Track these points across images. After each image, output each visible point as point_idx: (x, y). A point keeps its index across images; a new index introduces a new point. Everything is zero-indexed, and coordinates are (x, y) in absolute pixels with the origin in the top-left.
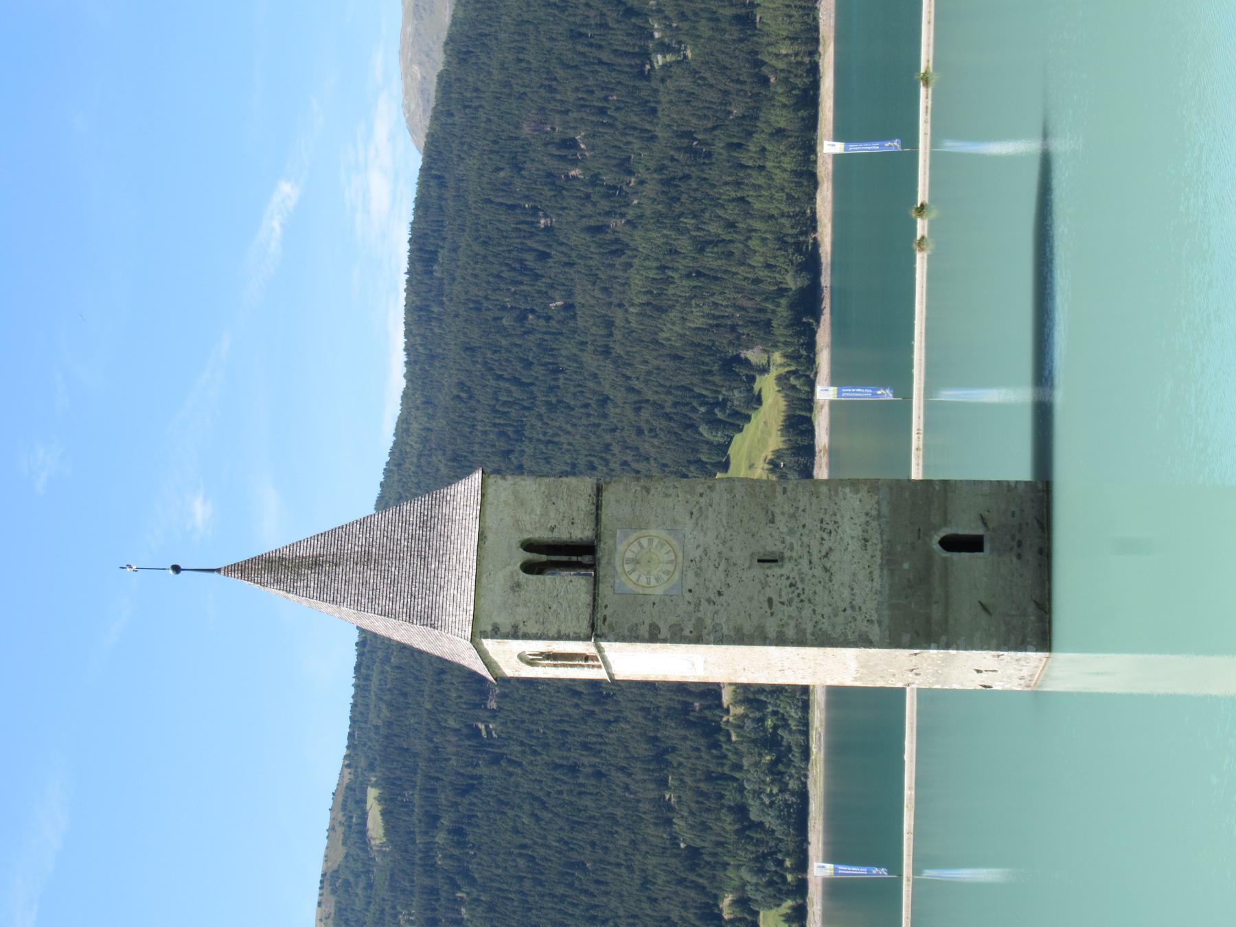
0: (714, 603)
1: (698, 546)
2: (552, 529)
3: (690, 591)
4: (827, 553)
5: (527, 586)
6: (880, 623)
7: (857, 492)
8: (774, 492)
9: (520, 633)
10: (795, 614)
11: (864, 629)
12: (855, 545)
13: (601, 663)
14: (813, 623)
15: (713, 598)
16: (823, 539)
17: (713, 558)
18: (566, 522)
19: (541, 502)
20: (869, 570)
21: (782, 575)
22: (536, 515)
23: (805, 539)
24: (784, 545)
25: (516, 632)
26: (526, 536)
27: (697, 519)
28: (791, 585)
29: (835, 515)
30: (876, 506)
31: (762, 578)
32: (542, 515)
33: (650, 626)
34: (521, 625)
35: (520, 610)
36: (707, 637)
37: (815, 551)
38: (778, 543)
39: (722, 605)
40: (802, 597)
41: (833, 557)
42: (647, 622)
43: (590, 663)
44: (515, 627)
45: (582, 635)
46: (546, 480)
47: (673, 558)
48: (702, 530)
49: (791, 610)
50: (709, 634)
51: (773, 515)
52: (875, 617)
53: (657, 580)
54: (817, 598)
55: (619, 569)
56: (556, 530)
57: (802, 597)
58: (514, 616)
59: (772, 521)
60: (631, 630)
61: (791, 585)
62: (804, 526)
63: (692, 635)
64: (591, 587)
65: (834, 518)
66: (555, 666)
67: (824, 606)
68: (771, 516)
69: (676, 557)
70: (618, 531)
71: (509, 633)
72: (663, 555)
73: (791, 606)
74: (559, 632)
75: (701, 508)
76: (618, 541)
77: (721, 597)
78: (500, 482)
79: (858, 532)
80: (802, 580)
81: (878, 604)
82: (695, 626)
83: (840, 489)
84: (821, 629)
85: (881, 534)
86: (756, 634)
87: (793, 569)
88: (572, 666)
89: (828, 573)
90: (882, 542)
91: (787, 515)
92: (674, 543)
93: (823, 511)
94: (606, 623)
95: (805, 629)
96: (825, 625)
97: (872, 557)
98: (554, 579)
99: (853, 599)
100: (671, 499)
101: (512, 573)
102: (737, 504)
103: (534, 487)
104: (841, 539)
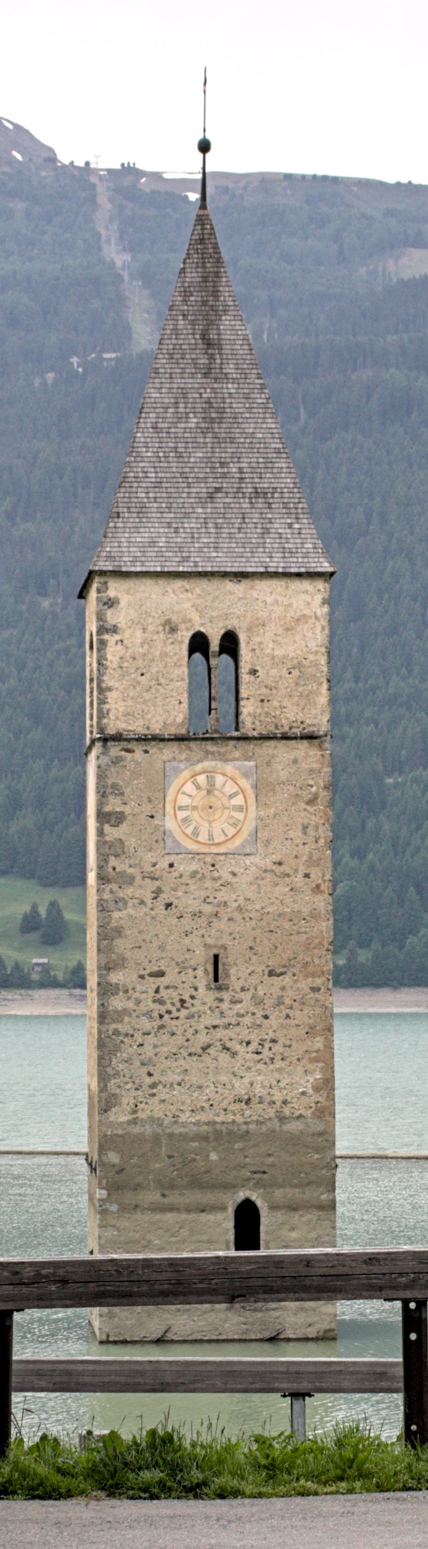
0: (155, 898)
1: (234, 874)
2: (253, 672)
3: (171, 865)
4: (228, 1049)
5: (172, 643)
6: (134, 1122)
7: (317, 1089)
8: (313, 975)
9: (106, 637)
10: (143, 1008)
11: (125, 1101)
12: (240, 1087)
14: (131, 1032)
15: (162, 896)
16: (248, 1043)
17: (219, 895)
18: (264, 691)
19: (291, 655)
20: (206, 1105)
21: (196, 989)
22: (273, 649)
23: (247, 1020)
24: (239, 990)
25: (107, 631)
26: (242, 638)
27: (272, 871)
28: (182, 1001)
29: (283, 1059)
30: (297, 1113)
31: (192, 963)
32: (273, 658)
33: (122, 813)
34: (117, 637)
35: (139, 634)
36: (108, 889)
37: (229, 1033)
38: (241, 983)
39: (152, 909)
40: (167, 1017)
41: (224, 1057)
42: (127, 810)
44: (115, 630)
45: (105, 721)
46: (323, 660)
47: (216, 841)
48: (257, 878)
49: (148, 1004)
50: (111, 892)
51: (281, 974)
52: (141, 1115)
53: (185, 820)
54: (166, 1037)
55: (199, 767)
56: (252, 678)
57: (167, 1017)
58: (130, 627)
59: (271, 974)
60: (115, 786)
61: (182, 1001)
62: (266, 1017)
63: (110, 870)
64: (173, 731)
65: (278, 1057)
67: (155, 1046)
68: (278, 971)
69: (219, 844)
70: (252, 763)
71: (106, 621)
72: (220, 827)
73: (154, 1001)
74: (109, 689)
75: (288, 875)
76: (238, 763)
77: (163, 908)
78: (319, 598)
79: (258, 1091)
80: (190, 1017)
81: (159, 1119)
82: (122, 874)
83: (320, 1065)
84: (122, 1042)
85: (258, 1122)
86: (113, 956)
87: (204, 1004)
89: (200, 1051)
90: (246, 1123)
91: (281, 993)
92: (238, 842)
93: (288, 1043)
94: (123, 753)
95: (122, 1021)
96: (129, 1049)
97: (225, 1110)
98: (183, 680)
99: (165, 1086)
100: (300, 834)
101: (190, 620)
102: (294, 925)
103: (313, 645)
104: (249, 1068)
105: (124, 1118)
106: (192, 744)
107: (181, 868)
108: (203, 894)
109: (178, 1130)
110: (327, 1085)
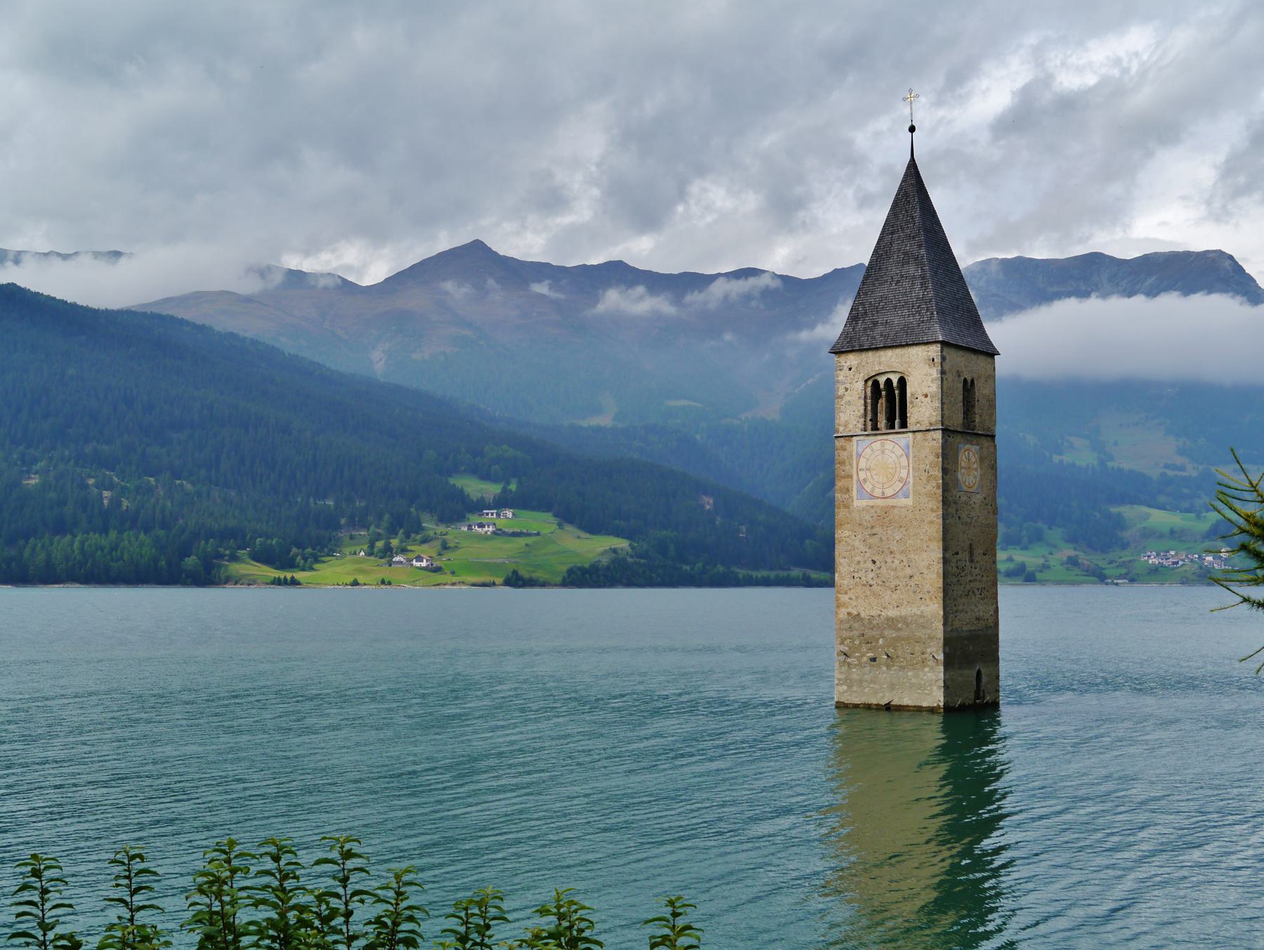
13: (869, 432)
41: (973, 597)
43: (869, 424)
59: (985, 554)
66: (865, 398)
70: (978, 447)
88: (865, 410)
105: (949, 629)
106: (965, 435)
107: (962, 498)
108: (966, 512)
109: (963, 634)
110: (997, 609)
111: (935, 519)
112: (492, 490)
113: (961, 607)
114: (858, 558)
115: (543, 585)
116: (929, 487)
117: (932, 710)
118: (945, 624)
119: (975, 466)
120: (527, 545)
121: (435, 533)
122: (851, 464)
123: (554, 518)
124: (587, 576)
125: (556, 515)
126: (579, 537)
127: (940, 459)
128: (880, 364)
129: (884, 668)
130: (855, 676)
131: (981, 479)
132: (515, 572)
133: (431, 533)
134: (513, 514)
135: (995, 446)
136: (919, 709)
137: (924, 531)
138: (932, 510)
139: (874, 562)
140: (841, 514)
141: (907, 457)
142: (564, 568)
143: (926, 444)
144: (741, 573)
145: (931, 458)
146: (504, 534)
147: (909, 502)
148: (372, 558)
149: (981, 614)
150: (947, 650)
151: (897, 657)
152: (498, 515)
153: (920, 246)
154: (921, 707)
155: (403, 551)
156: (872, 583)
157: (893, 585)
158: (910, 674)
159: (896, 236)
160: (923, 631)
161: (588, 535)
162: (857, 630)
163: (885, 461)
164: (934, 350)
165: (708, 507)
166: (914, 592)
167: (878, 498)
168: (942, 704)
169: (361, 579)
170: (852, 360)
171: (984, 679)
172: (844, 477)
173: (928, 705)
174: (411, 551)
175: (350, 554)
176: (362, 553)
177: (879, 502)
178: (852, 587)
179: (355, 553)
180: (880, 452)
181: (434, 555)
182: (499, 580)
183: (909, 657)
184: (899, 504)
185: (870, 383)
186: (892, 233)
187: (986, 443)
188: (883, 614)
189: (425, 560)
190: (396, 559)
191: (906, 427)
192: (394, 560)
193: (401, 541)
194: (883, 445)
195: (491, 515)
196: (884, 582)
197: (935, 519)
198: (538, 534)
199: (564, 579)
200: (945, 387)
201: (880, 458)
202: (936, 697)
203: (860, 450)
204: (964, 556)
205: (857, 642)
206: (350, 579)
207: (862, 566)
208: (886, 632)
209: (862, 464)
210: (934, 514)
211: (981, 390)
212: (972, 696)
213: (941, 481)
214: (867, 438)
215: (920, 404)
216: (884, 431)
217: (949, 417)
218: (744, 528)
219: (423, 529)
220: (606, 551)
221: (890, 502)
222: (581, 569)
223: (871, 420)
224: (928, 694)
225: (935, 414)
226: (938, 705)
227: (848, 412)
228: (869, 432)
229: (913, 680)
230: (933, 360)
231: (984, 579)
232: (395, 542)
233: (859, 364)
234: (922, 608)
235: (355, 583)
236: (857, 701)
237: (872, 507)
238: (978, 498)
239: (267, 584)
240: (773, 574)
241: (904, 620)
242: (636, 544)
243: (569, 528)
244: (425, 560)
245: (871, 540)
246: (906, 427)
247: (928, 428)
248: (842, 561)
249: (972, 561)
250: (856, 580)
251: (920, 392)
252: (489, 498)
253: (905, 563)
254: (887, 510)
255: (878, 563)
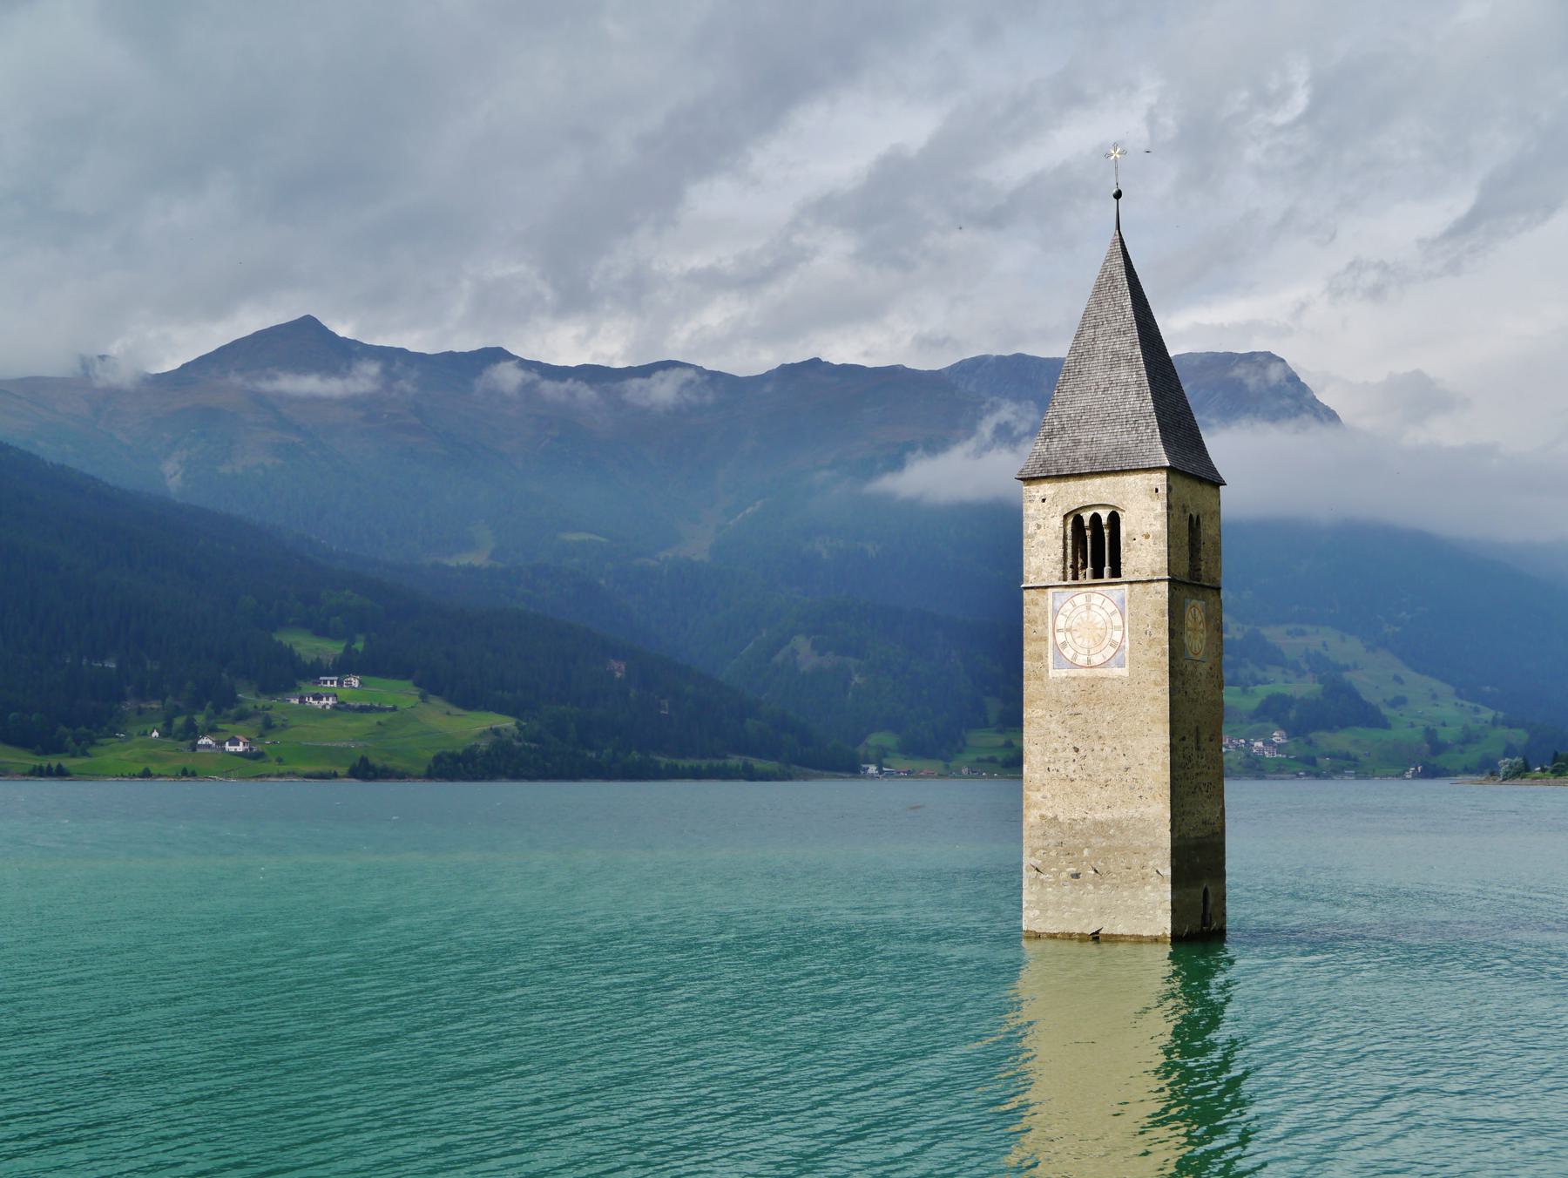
13: (1070, 582)
43: (1070, 571)
59: (1211, 740)
69: (1196, 654)
111: (1159, 694)
112: (332, 649)
113: (1188, 809)
114: (1055, 745)
115: (401, 776)
116: (1151, 654)
117: (1155, 940)
118: (1172, 830)
119: (1201, 627)
120: (379, 723)
121: (256, 707)
122: (1045, 624)
123: (415, 688)
124: (461, 764)
125: (418, 684)
126: (448, 714)
127: (1167, 618)
128: (1085, 494)
129: (1091, 887)
130: (1052, 897)
131: (1207, 644)
132: (364, 760)
133: (249, 707)
134: (360, 682)
135: (1221, 601)
136: (1139, 940)
137: (1145, 710)
138: (1156, 683)
139: (1077, 750)
140: (1030, 688)
141: (1122, 614)
142: (429, 755)
143: (1148, 598)
144: (663, 761)
145: (1154, 616)
146: (349, 708)
147: (1124, 672)
148: (169, 740)
149: (1208, 816)
150: (1174, 864)
151: (1109, 872)
152: (340, 683)
153: (1133, 344)
154: (1141, 936)
155: (211, 731)
156: (1074, 777)
157: (1102, 780)
158: (1125, 894)
159: (1100, 331)
160: (1144, 838)
161: (460, 711)
162: (1053, 838)
163: (1091, 619)
164: (1160, 479)
165: (618, 675)
166: (1132, 788)
167: (1082, 667)
168: (1169, 933)
169: (154, 768)
170: (1047, 489)
171: (1211, 901)
172: (1035, 640)
173: (1149, 934)
174: (222, 731)
175: (139, 735)
176: (155, 734)
177: (1083, 672)
178: (1045, 782)
179: (145, 734)
180: (1084, 608)
181: (253, 736)
182: (342, 770)
183: (1124, 872)
184: (1111, 675)
185: (1070, 520)
186: (1095, 327)
187: (1210, 594)
188: (1089, 817)
189: (241, 744)
190: (204, 741)
191: (1120, 576)
192: (199, 742)
193: (209, 718)
194: (1088, 599)
195: (331, 683)
196: (1090, 775)
197: (1159, 694)
198: (394, 709)
199: (429, 769)
200: (1171, 526)
201: (1084, 615)
202: (1163, 924)
203: (1058, 604)
204: (1191, 742)
205: (1053, 853)
206: (140, 768)
207: (1061, 755)
208: (1093, 840)
209: (1061, 622)
210: (1158, 689)
211: (1207, 530)
212: (1199, 922)
213: (1168, 646)
214: (1067, 590)
215: (1139, 546)
216: (1089, 580)
217: (1175, 564)
218: (666, 703)
219: (238, 701)
220: (485, 732)
221: (1100, 672)
222: (452, 756)
223: (1071, 567)
224: (1151, 920)
225: (1159, 559)
226: (1164, 934)
227: (1041, 556)
228: (1070, 582)
229: (1130, 902)
230: (1157, 490)
231: (1211, 771)
232: (200, 719)
233: (1056, 495)
234: (1141, 809)
235: (146, 774)
236: (1053, 930)
237: (1074, 678)
238: (1204, 668)
239: (24, 775)
240: (704, 764)
241: (1118, 824)
242: (524, 724)
243: (436, 701)
244: (241, 744)
245: (1072, 722)
246: (1119, 575)
247: (1150, 578)
248: (1033, 748)
249: (1198, 749)
250: (1051, 773)
251: (1139, 532)
252: (328, 661)
253: (1119, 752)
254: (1094, 683)
255: (1082, 752)
